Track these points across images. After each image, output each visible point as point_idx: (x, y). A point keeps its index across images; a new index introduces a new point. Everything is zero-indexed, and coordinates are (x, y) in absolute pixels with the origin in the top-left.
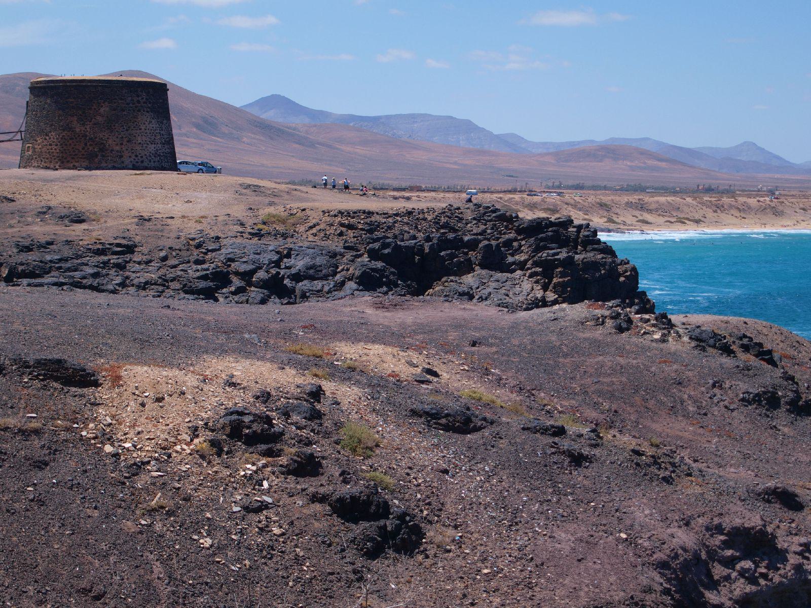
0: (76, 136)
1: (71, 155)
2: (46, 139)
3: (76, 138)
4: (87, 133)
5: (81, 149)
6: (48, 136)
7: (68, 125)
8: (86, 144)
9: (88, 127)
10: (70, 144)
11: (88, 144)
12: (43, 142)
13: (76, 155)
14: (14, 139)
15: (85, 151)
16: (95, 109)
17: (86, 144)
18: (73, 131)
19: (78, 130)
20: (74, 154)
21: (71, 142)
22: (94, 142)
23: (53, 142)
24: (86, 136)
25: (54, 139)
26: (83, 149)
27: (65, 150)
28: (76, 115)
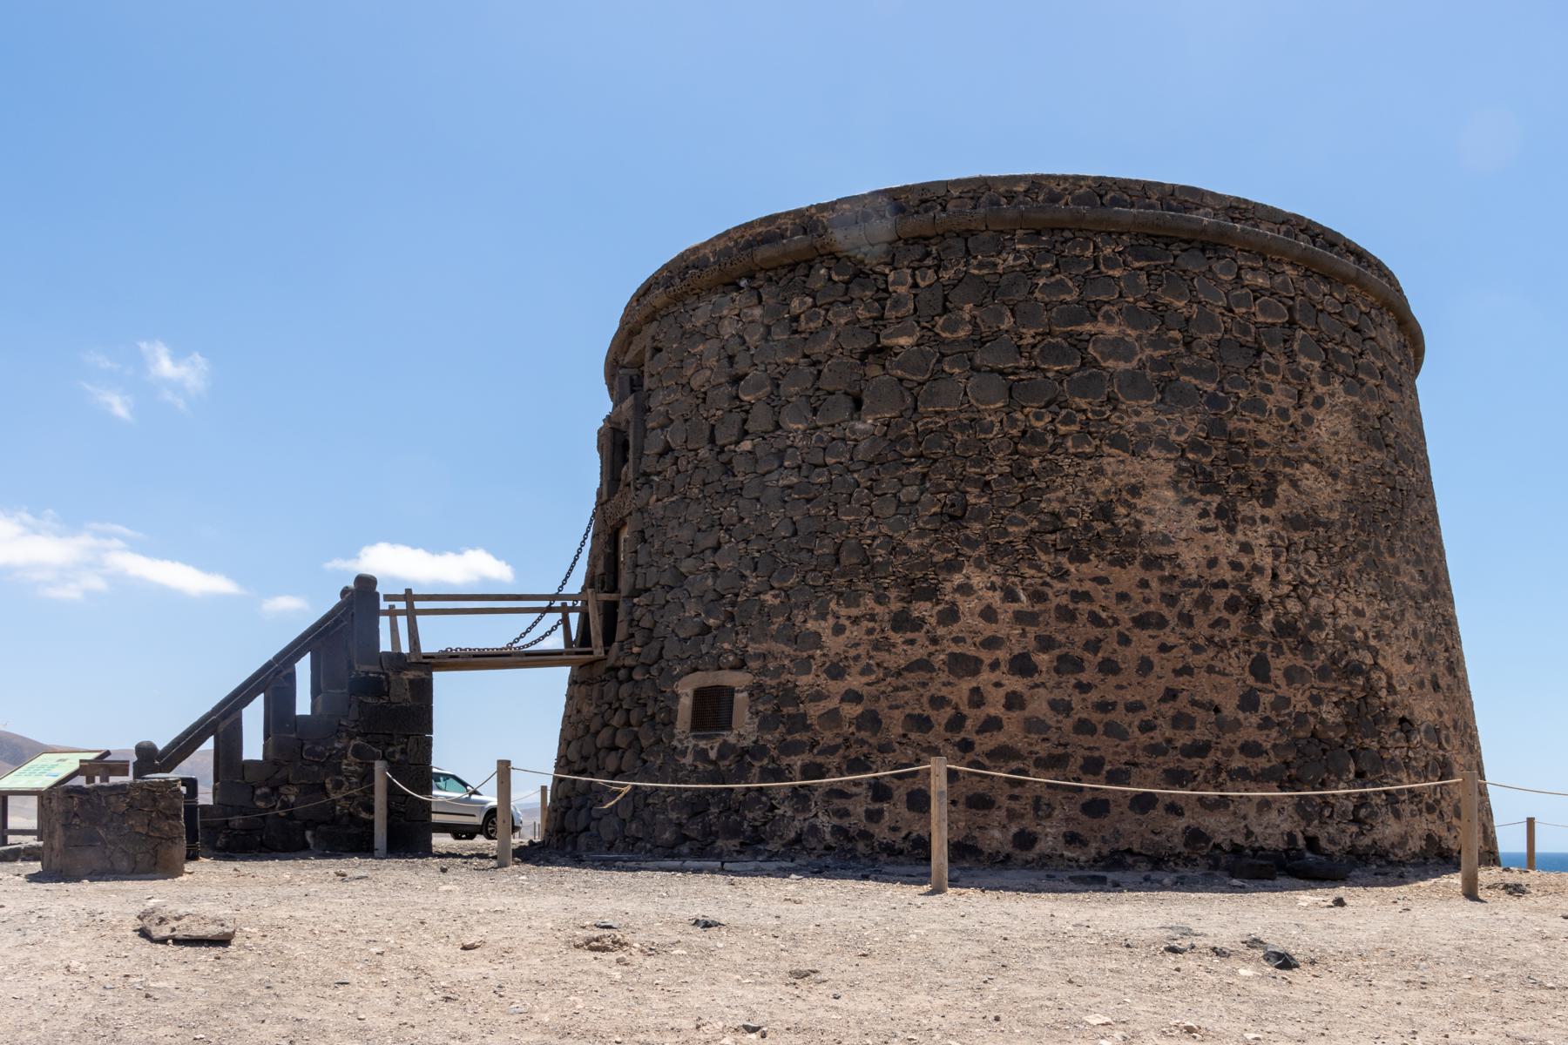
0: (1186, 602)
1: (1154, 750)
2: (902, 622)
3: (1186, 619)
4: (1261, 585)
5: (1230, 709)
6: (931, 594)
7: (1105, 512)
8: (1260, 668)
9: (1259, 536)
10: (1145, 666)
11: (1278, 665)
12: (883, 645)
13: (1200, 749)
14: (538, 615)
15: (1266, 724)
16: (1283, 413)
17: (1260, 668)
18: (1151, 563)
19: (1191, 558)
20: (1183, 738)
21: (1144, 643)
22: (1306, 647)
23: (992, 643)
24: (1256, 603)
25: (989, 614)
26: (1249, 702)
27: (1104, 707)
28: (1164, 444)
